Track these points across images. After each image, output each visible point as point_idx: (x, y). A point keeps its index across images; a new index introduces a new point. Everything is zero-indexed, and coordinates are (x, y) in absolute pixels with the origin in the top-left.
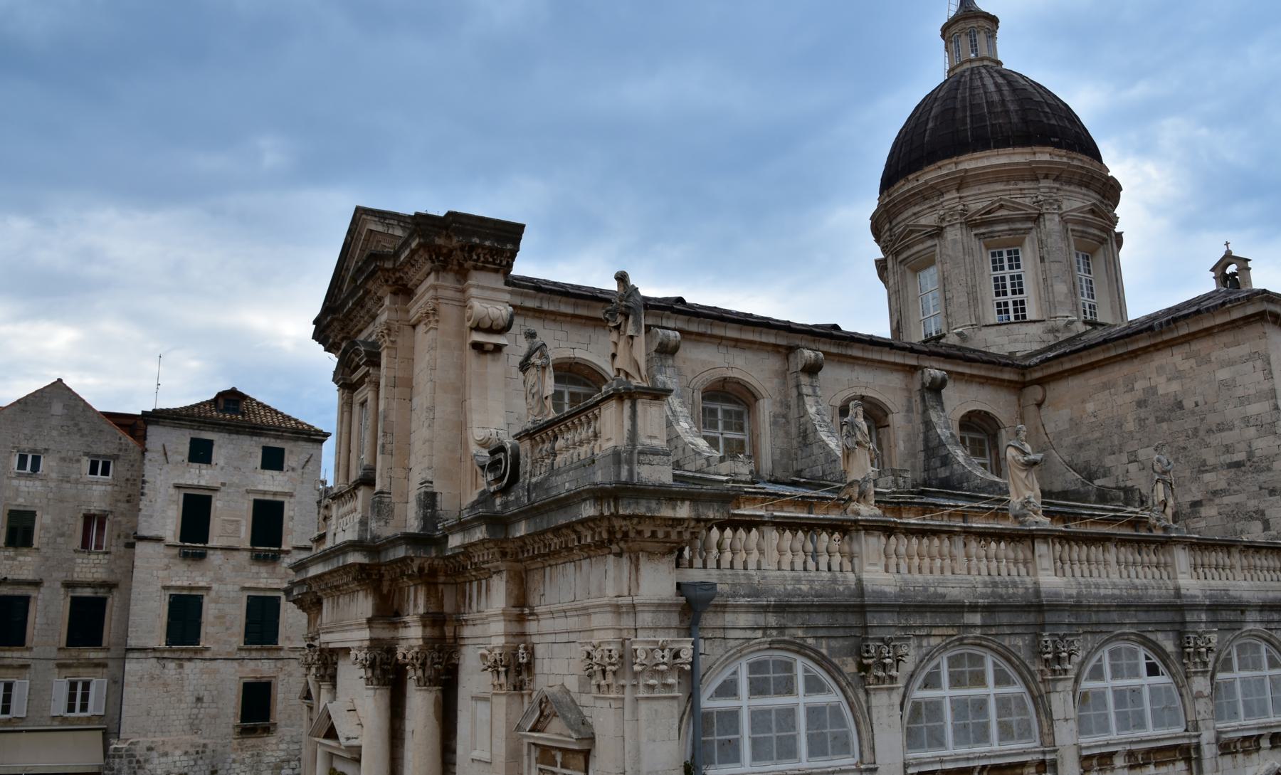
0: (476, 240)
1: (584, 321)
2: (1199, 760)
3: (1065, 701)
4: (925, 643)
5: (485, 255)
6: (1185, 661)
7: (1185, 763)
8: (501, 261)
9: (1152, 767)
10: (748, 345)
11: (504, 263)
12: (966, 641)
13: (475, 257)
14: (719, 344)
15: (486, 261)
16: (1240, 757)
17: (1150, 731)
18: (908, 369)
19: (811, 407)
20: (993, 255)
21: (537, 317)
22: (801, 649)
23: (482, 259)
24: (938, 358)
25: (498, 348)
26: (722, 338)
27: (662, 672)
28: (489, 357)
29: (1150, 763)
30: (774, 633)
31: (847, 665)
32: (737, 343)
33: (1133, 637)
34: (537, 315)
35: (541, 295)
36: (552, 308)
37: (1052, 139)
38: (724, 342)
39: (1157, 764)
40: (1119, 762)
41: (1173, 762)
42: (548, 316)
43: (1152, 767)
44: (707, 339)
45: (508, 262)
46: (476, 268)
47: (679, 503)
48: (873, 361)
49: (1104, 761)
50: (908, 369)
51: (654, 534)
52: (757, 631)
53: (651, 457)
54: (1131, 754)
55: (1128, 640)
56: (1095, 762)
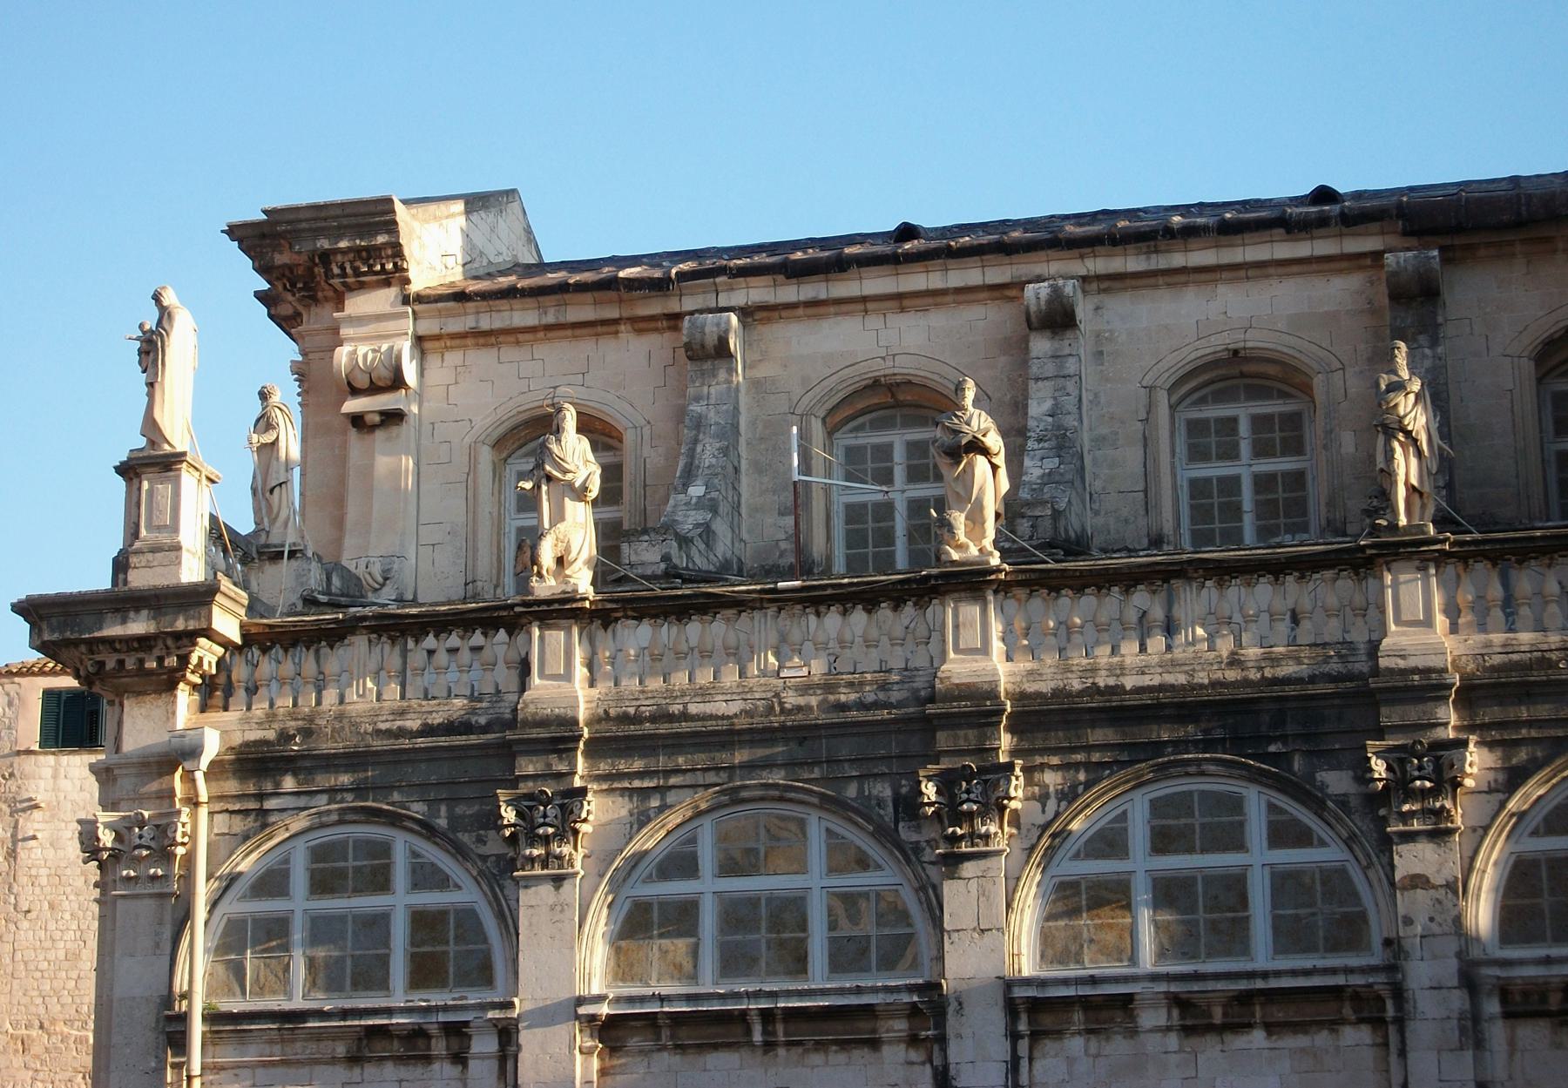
0: (323, 244)
1: (569, 332)
2: (1400, 1022)
3: (982, 893)
5: (351, 262)
6: (1382, 812)
7: (1374, 1030)
8: (383, 266)
9: (1258, 1037)
10: (930, 300)
11: (390, 266)
12: (744, 794)
13: (336, 271)
14: (866, 311)
15: (365, 274)
17: (1262, 954)
18: (1369, 262)
19: (1041, 401)
21: (485, 345)
22: (394, 820)
23: (349, 270)
24: (1266, 235)
25: (393, 418)
26: (864, 299)
27: (140, 859)
28: (379, 435)
29: (1249, 1026)
30: (349, 797)
31: (485, 843)
32: (900, 301)
33: (1212, 768)
34: (482, 341)
35: (470, 305)
36: (497, 325)
38: (870, 306)
39: (1271, 1028)
40: (1151, 1018)
41: (1334, 1025)
42: (501, 339)
44: (832, 309)
45: (395, 264)
46: (350, 288)
47: (132, 614)
48: (1184, 270)
49: (1104, 1014)
50: (1369, 262)
51: (121, 663)
52: (319, 796)
53: (150, 556)
54: (1176, 1001)
55: (1202, 774)
56: (1078, 1016)
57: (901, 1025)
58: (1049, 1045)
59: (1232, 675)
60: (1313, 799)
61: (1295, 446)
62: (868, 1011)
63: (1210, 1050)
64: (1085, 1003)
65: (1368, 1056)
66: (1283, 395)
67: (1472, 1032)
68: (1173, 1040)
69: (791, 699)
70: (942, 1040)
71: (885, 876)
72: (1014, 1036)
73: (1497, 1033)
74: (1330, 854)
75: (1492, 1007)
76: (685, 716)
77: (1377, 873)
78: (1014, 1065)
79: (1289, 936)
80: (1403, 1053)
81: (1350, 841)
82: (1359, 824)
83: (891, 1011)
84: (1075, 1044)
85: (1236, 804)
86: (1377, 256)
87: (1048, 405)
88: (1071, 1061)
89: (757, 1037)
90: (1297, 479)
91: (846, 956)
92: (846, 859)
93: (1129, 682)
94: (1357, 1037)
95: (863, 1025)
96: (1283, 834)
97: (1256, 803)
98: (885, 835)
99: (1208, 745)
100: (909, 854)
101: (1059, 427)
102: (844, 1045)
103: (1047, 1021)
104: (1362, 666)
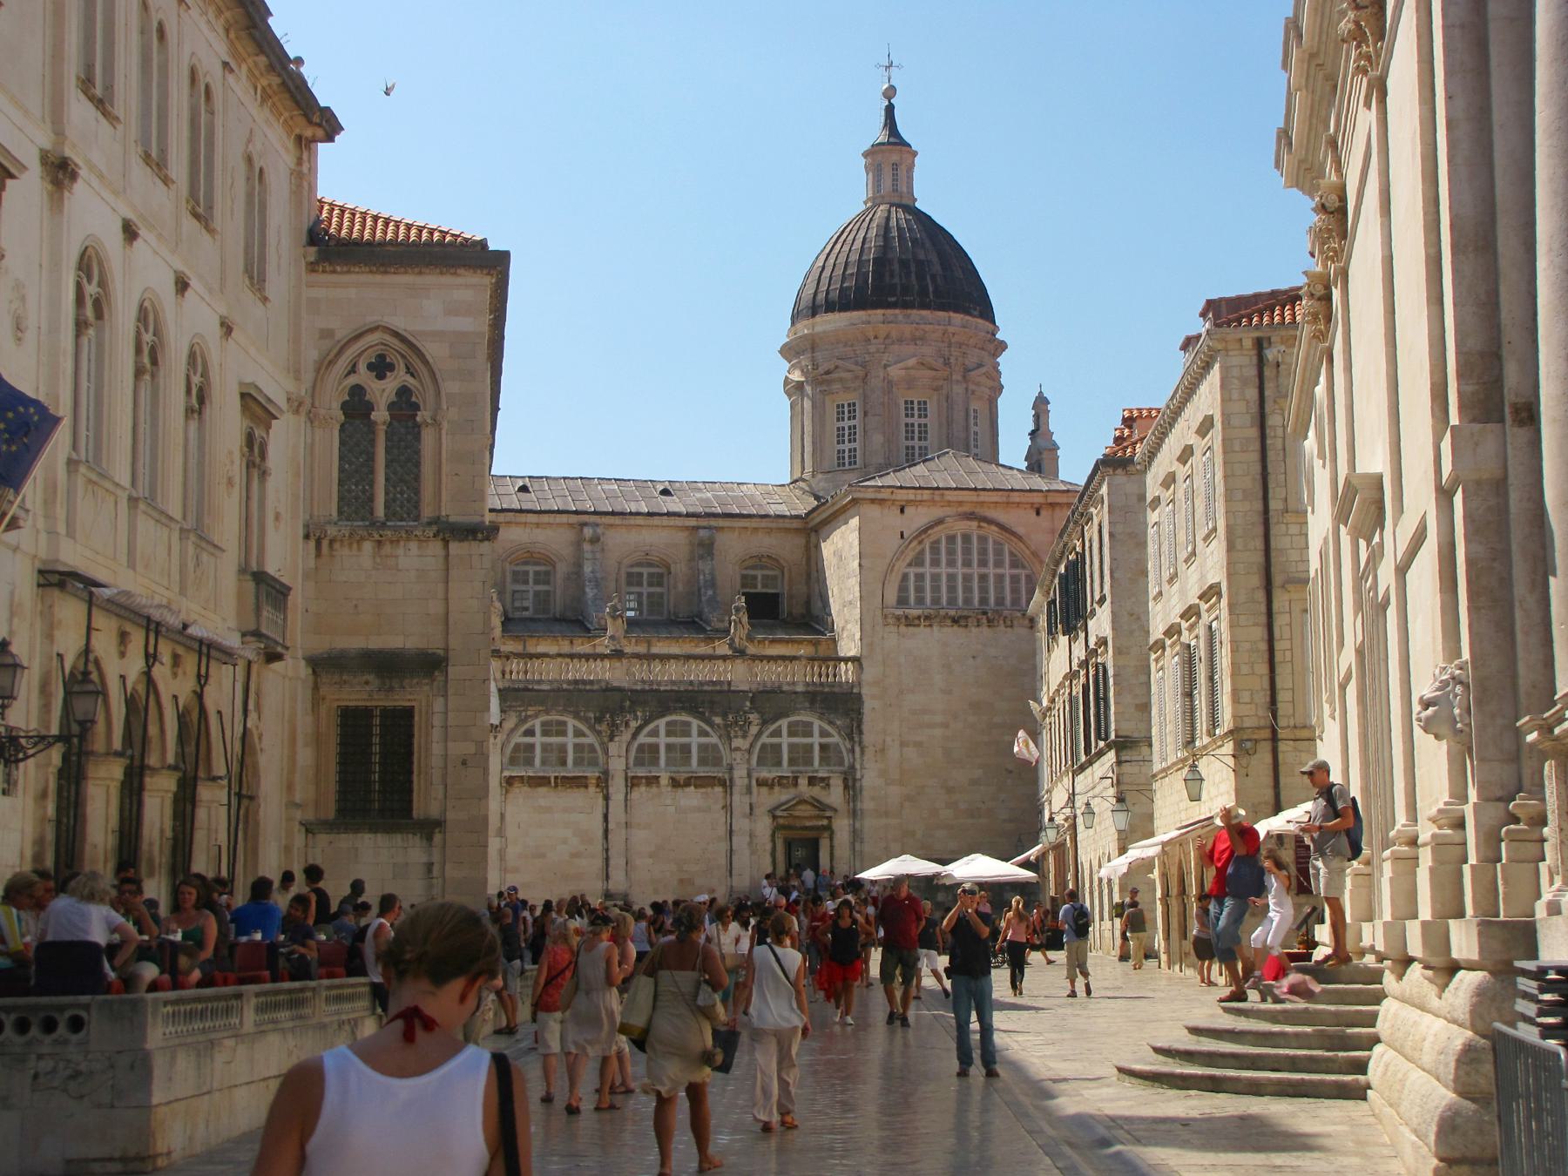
4: (523, 714)
9: (692, 788)
16: (777, 789)
20: (838, 406)
32: (538, 525)
37: (889, 299)
39: (696, 787)
41: (713, 786)
43: (692, 788)
56: (644, 781)
57: (594, 781)
58: (636, 789)
59: (690, 688)
60: (711, 724)
61: (660, 584)
62: (586, 777)
63: (680, 790)
64: (647, 778)
65: (722, 795)
66: (658, 566)
67: (749, 790)
68: (669, 789)
69: (565, 686)
70: (607, 787)
71: (590, 739)
72: (627, 786)
73: (755, 788)
74: (714, 739)
75: (754, 782)
76: (533, 690)
77: (727, 746)
78: (627, 793)
79: (703, 761)
80: (731, 795)
81: (720, 737)
82: (723, 732)
83: (591, 778)
84: (643, 789)
85: (688, 724)
86: (696, 528)
87: (590, 569)
88: (641, 793)
89: (553, 784)
90: (661, 595)
91: (578, 762)
92: (578, 733)
93: (662, 688)
94: (719, 789)
95: (583, 781)
96: (702, 733)
97: (695, 723)
98: (592, 728)
99: (683, 708)
100: (599, 733)
101: (595, 577)
102: (578, 787)
103: (635, 781)
104: (726, 688)
